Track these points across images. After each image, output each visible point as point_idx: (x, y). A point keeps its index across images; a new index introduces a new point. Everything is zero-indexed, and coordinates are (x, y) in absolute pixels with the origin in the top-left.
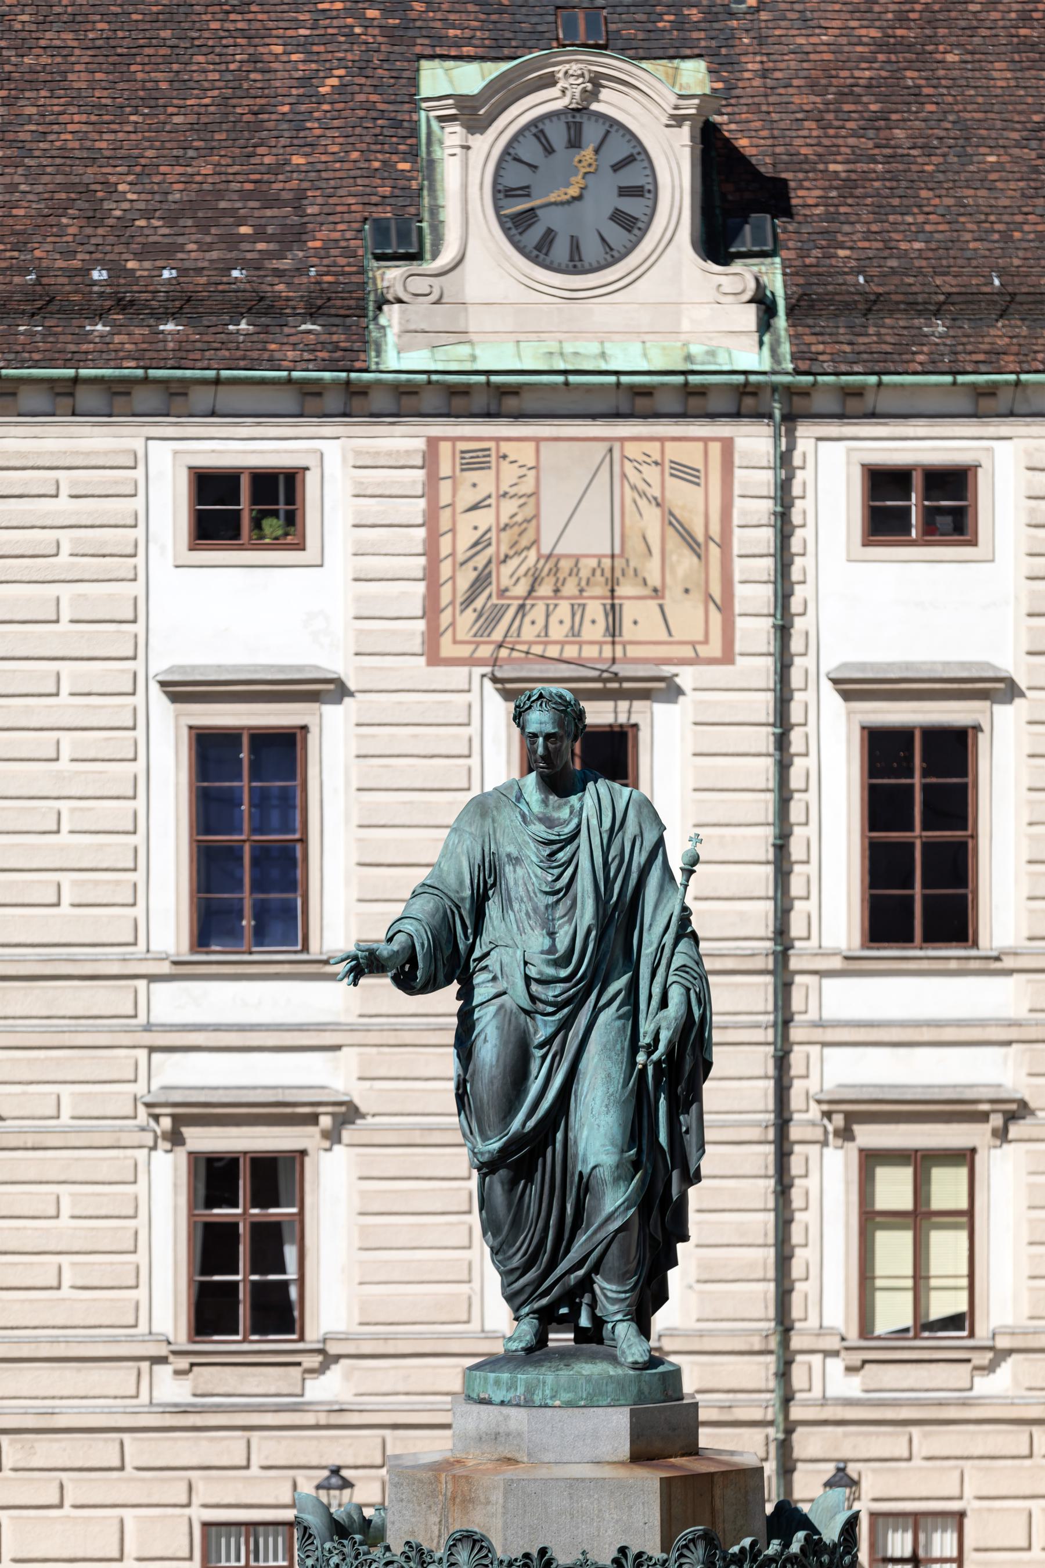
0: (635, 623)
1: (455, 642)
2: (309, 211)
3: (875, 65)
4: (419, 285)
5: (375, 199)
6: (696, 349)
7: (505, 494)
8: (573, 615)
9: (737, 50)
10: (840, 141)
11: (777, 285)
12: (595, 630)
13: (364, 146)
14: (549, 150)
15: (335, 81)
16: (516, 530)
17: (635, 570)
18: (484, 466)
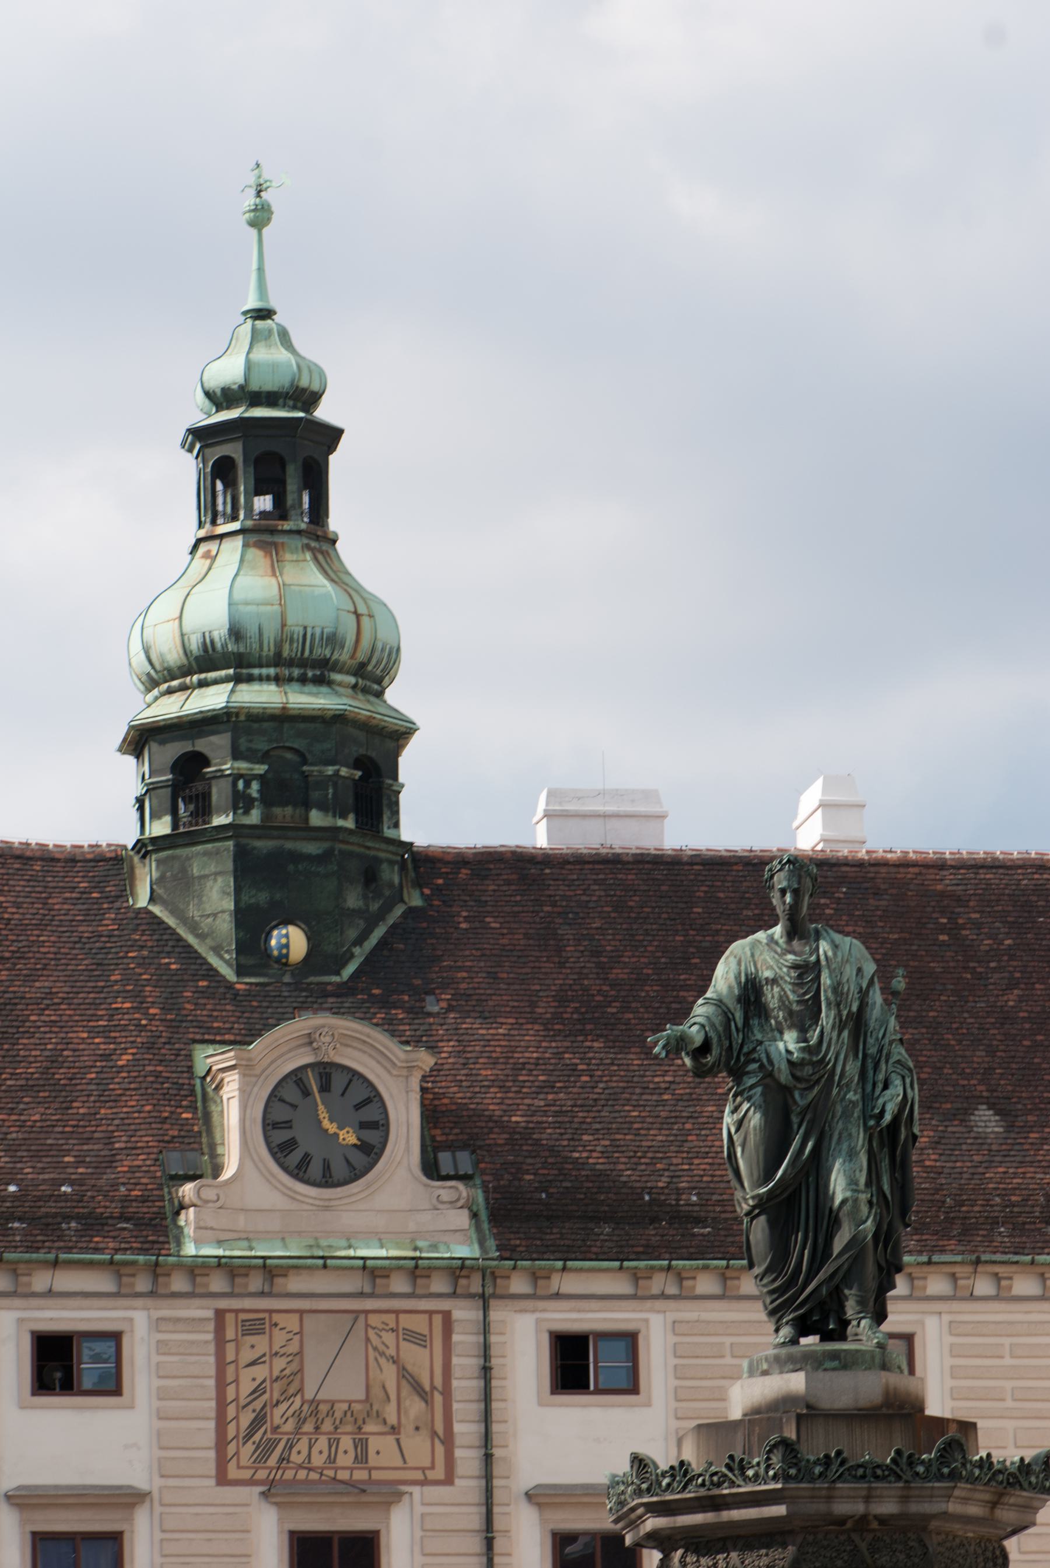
0: (378, 1453)
1: (239, 1467)
2: (117, 1146)
3: (540, 1050)
4: (209, 1194)
5: (166, 1138)
6: (420, 1244)
7: (276, 1354)
8: (330, 1447)
9: (435, 1038)
10: (518, 1101)
12: (345, 1460)
13: (155, 1102)
15: (130, 1057)
16: (285, 1381)
17: (377, 1412)
18: (260, 1332)
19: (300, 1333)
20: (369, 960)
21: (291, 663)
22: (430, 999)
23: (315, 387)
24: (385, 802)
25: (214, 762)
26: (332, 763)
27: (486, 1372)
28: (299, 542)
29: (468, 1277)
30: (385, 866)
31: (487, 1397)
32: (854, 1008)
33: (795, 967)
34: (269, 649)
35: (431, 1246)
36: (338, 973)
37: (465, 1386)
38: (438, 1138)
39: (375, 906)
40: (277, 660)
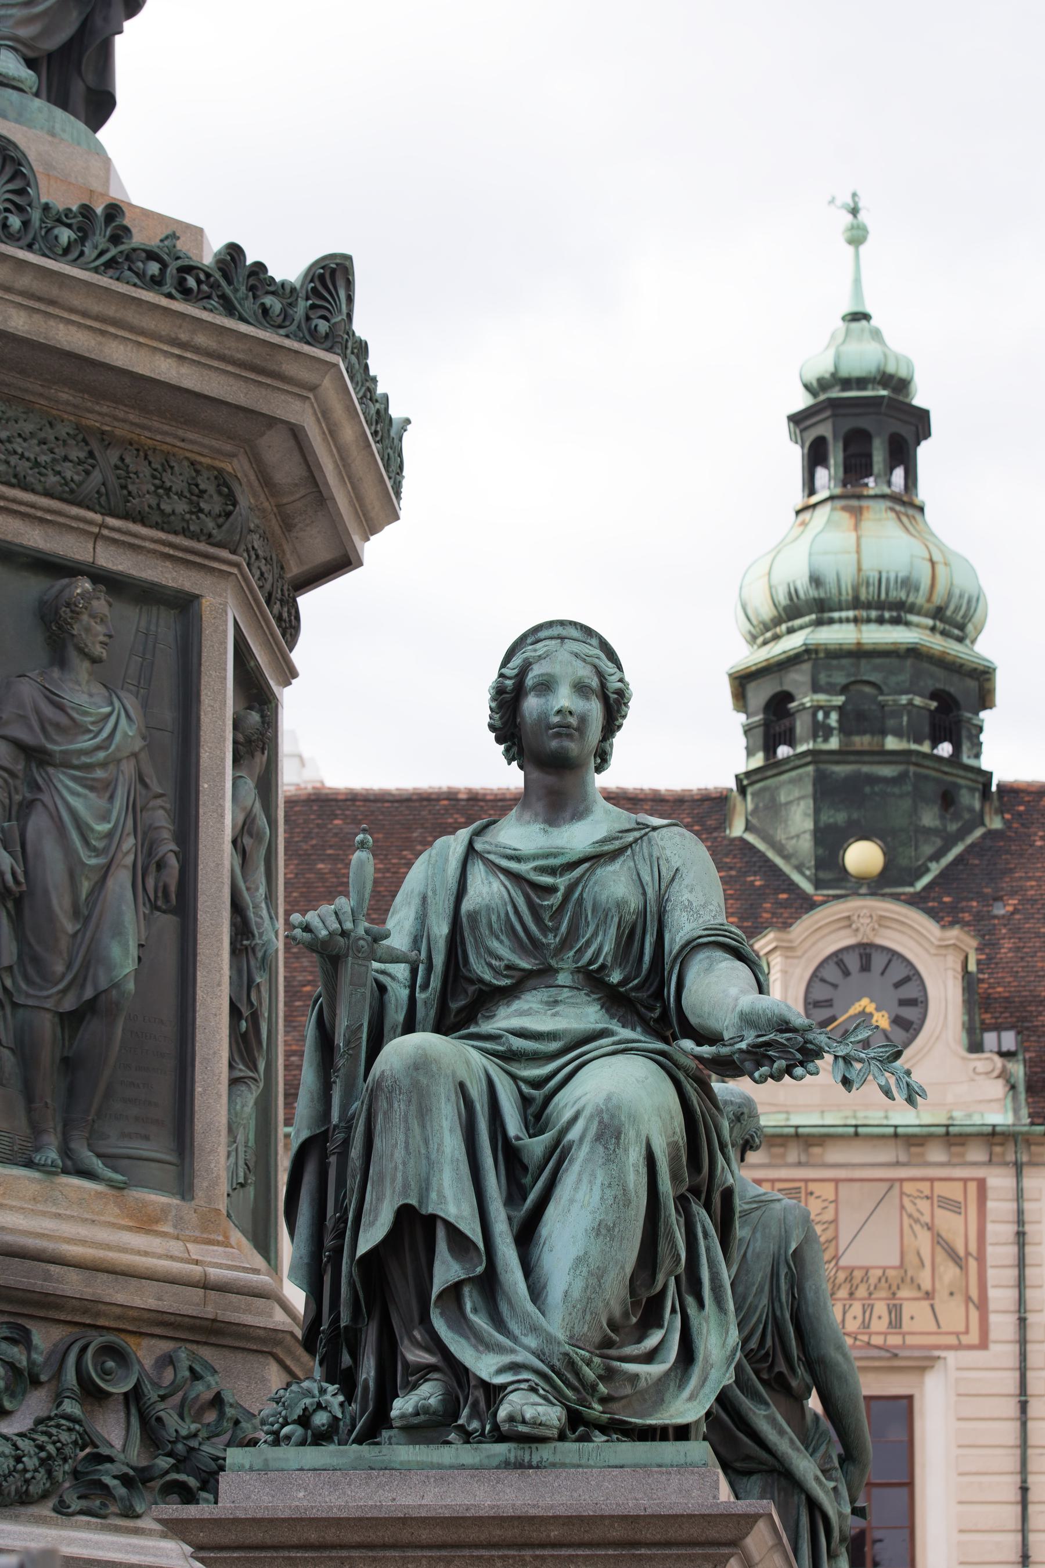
0: (912, 1318)
6: (955, 1114)
8: (864, 1312)
11: (1018, 1070)
12: (879, 1325)
14: (846, 973)
17: (912, 1279)
19: (836, 1201)
20: (943, 874)
21: (868, 606)
22: (1000, 904)
23: (903, 373)
24: (964, 733)
25: (798, 697)
26: (906, 693)
27: (1021, 1237)
29: (1002, 1144)
30: (964, 792)
31: (1021, 1263)
34: (847, 595)
35: (965, 1116)
36: (912, 885)
37: (1000, 1252)
38: (987, 1021)
39: (953, 827)
40: (856, 603)
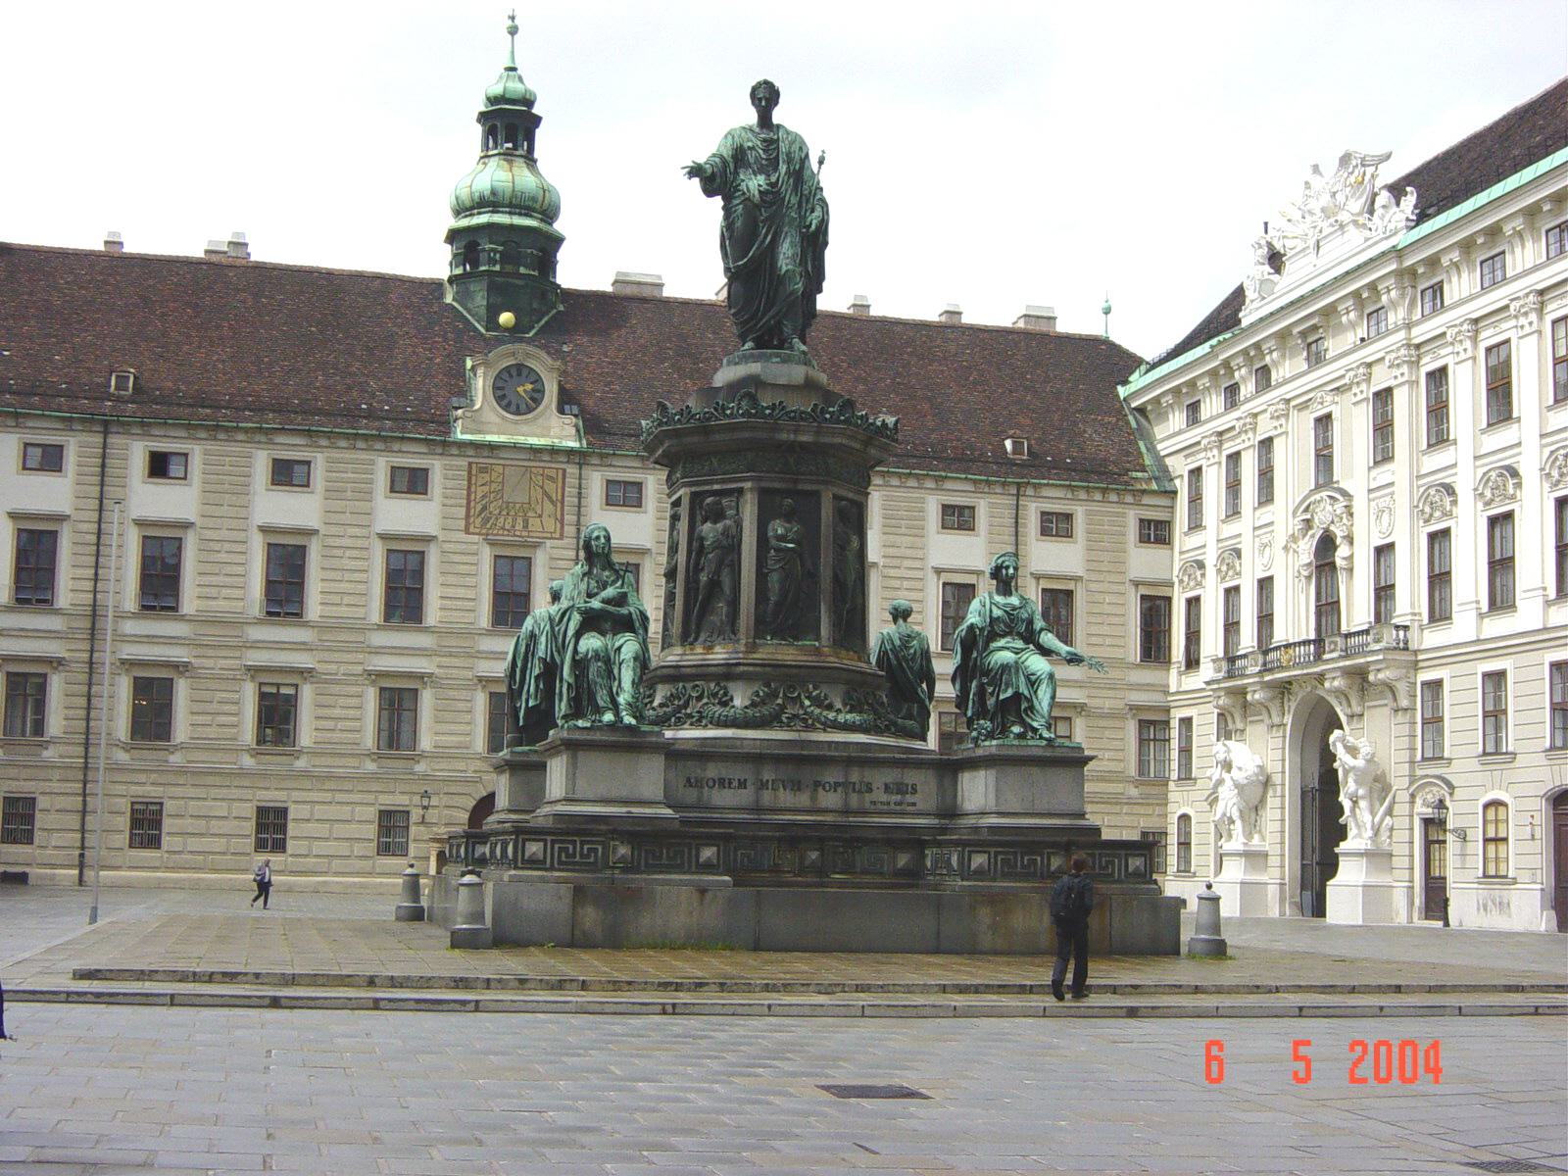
12: (519, 526)
14: (511, 376)
28: (522, 160)
31: (579, 507)
32: (797, 167)
33: (764, 140)
34: (507, 202)
37: (571, 500)
40: (510, 205)
